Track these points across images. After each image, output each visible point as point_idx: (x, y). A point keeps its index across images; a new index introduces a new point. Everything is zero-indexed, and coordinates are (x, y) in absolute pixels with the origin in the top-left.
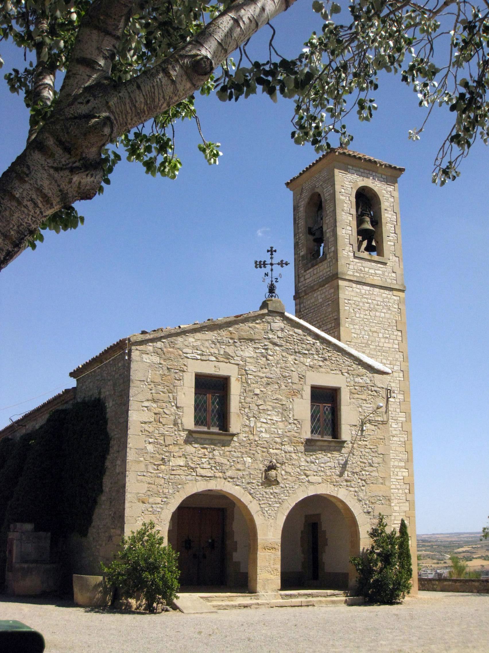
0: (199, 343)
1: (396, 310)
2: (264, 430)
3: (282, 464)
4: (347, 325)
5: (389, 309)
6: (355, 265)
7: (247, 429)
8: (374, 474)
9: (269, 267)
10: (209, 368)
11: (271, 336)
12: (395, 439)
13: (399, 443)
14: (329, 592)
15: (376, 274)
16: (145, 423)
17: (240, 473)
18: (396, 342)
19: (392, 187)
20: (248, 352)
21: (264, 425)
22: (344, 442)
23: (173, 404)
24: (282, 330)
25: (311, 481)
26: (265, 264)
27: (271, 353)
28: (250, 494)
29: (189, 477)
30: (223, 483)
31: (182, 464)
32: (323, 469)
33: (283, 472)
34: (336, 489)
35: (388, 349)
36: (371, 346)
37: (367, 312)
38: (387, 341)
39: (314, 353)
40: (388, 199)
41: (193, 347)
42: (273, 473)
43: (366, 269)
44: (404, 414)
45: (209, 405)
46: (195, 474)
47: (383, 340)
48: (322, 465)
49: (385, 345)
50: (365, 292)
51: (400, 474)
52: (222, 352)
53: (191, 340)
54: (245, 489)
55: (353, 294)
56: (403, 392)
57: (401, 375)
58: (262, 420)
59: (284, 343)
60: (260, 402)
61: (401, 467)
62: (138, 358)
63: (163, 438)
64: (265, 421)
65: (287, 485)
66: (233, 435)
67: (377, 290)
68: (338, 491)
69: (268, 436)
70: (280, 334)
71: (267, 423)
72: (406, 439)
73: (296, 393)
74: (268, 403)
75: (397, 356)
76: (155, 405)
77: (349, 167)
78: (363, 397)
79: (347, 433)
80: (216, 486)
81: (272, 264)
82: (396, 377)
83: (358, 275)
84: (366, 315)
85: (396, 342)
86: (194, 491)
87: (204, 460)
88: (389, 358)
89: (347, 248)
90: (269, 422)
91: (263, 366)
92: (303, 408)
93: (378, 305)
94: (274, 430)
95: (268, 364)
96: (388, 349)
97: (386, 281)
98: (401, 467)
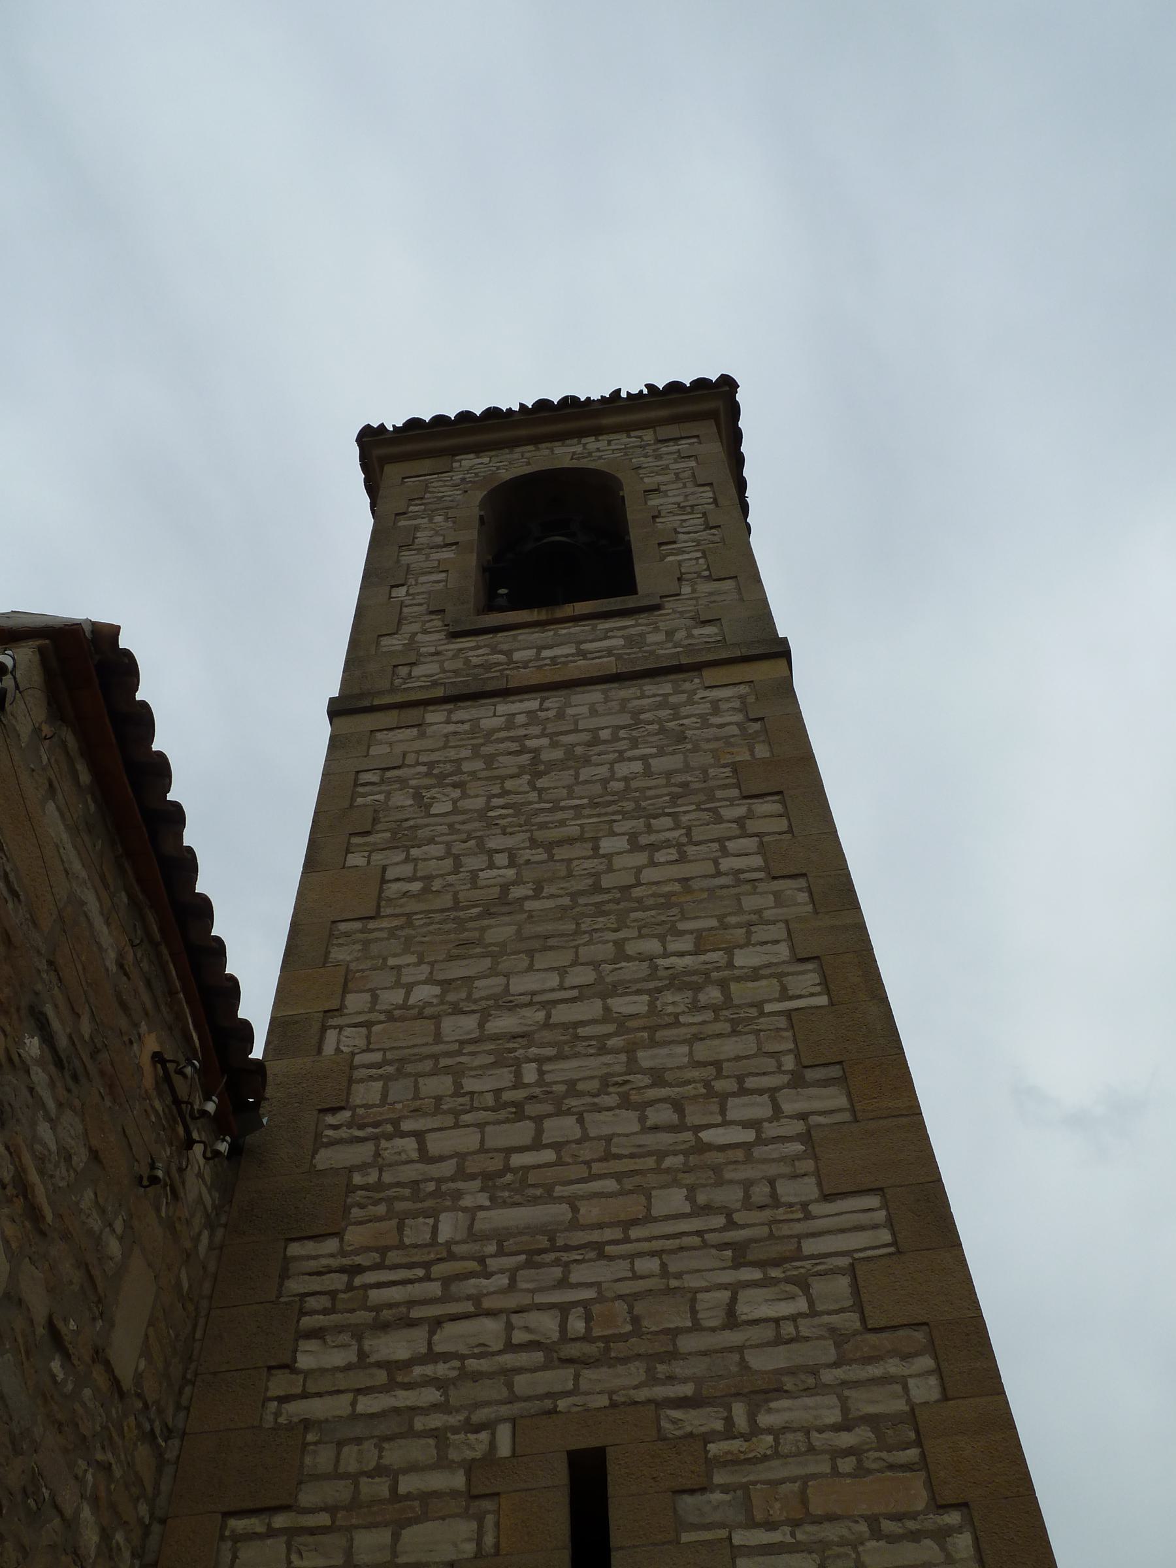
13: (846, 1439)
35: (677, 887)
44: (874, 1201)
56: (835, 1072)
57: (806, 980)
72: (925, 1390)
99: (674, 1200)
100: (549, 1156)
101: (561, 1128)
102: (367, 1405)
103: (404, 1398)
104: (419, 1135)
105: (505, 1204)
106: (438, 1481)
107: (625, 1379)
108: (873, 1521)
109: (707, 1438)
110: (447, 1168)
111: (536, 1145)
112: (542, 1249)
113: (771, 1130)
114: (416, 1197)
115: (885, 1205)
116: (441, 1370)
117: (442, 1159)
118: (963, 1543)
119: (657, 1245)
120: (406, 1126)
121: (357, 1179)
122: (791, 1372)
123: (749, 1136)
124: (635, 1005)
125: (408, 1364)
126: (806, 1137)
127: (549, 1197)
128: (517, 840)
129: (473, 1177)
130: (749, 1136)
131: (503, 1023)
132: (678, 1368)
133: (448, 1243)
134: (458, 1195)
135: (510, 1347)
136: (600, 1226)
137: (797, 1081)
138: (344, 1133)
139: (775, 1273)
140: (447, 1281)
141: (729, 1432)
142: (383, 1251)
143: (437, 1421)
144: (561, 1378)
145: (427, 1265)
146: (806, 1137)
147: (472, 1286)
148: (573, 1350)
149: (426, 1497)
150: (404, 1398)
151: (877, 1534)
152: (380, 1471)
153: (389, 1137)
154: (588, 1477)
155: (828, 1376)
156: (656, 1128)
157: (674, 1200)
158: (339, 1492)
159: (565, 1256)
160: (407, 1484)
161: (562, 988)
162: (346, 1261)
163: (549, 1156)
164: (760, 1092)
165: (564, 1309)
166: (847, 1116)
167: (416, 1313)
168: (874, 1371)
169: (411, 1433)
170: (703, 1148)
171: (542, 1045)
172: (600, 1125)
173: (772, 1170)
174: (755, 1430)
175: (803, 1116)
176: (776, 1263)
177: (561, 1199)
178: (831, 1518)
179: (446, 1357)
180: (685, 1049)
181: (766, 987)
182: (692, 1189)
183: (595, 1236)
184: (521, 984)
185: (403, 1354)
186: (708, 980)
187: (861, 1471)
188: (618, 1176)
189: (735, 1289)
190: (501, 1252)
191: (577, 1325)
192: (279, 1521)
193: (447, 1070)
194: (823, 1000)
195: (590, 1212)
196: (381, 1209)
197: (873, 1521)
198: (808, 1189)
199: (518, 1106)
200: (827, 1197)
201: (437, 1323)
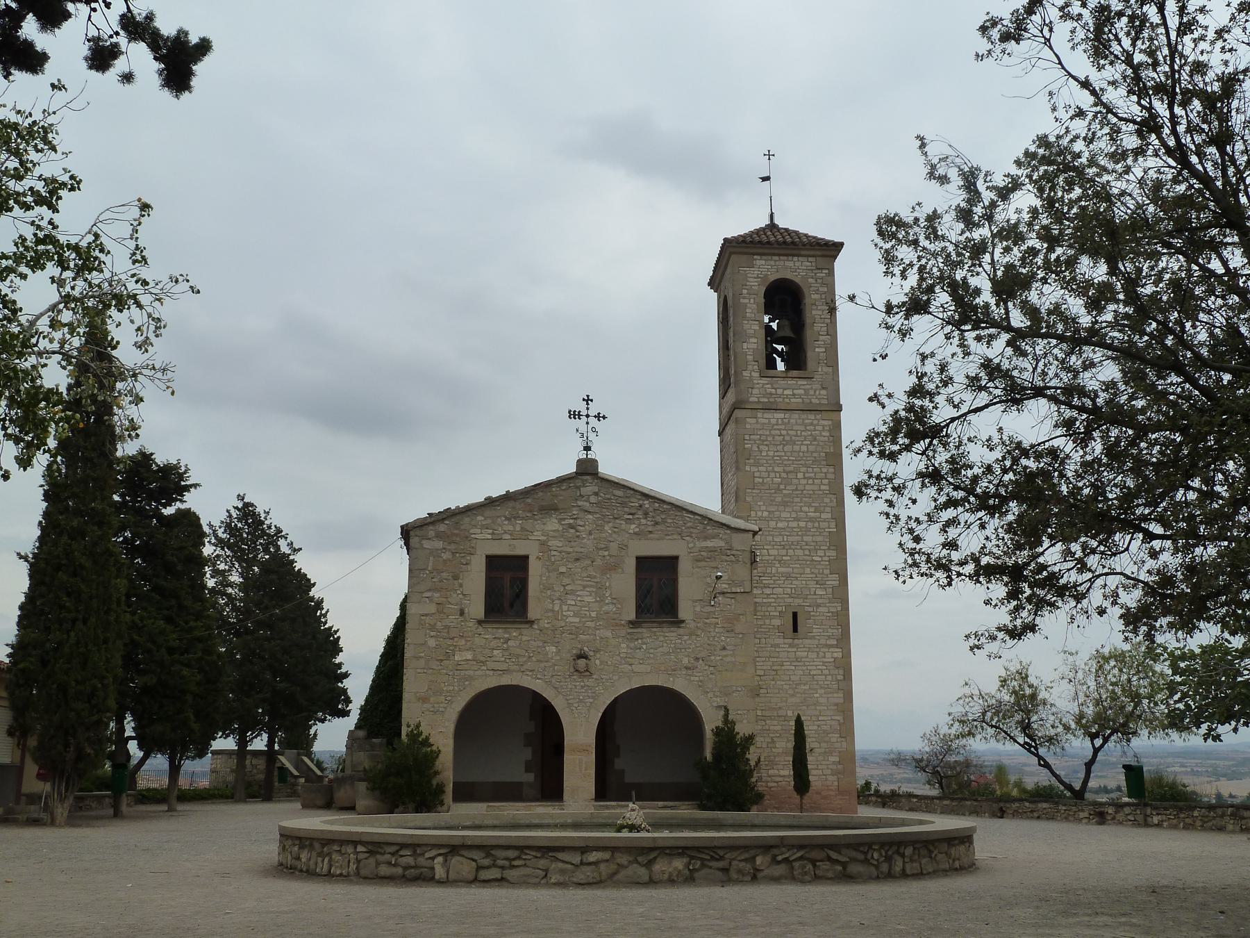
0: (489, 521)
3: (597, 651)
4: (748, 468)
5: (815, 439)
8: (729, 659)
9: (584, 418)
10: (500, 549)
11: (580, 503)
12: (821, 609)
14: (661, 804)
16: (426, 615)
17: (542, 665)
20: (552, 524)
22: (683, 621)
24: (596, 494)
26: (579, 415)
29: (479, 673)
31: (470, 657)
33: (598, 662)
38: (810, 481)
42: (582, 662)
43: (779, 391)
47: (804, 482)
49: (807, 487)
51: (828, 655)
52: (518, 528)
53: (480, 518)
55: (758, 426)
57: (833, 524)
59: (597, 509)
60: (566, 581)
61: (832, 646)
62: (417, 546)
66: (532, 622)
67: (796, 415)
70: (593, 499)
73: (612, 567)
75: (827, 500)
76: (437, 595)
78: (713, 564)
79: (684, 611)
81: (588, 416)
85: (826, 481)
89: (750, 367)
92: (625, 584)
98: (832, 646)
99: (808, 571)
101: (791, 552)
107: (799, 601)
112: (788, 576)
124: (802, 524)
131: (780, 525)
154: (795, 615)
157: (808, 571)
181: (826, 524)
184: (784, 515)
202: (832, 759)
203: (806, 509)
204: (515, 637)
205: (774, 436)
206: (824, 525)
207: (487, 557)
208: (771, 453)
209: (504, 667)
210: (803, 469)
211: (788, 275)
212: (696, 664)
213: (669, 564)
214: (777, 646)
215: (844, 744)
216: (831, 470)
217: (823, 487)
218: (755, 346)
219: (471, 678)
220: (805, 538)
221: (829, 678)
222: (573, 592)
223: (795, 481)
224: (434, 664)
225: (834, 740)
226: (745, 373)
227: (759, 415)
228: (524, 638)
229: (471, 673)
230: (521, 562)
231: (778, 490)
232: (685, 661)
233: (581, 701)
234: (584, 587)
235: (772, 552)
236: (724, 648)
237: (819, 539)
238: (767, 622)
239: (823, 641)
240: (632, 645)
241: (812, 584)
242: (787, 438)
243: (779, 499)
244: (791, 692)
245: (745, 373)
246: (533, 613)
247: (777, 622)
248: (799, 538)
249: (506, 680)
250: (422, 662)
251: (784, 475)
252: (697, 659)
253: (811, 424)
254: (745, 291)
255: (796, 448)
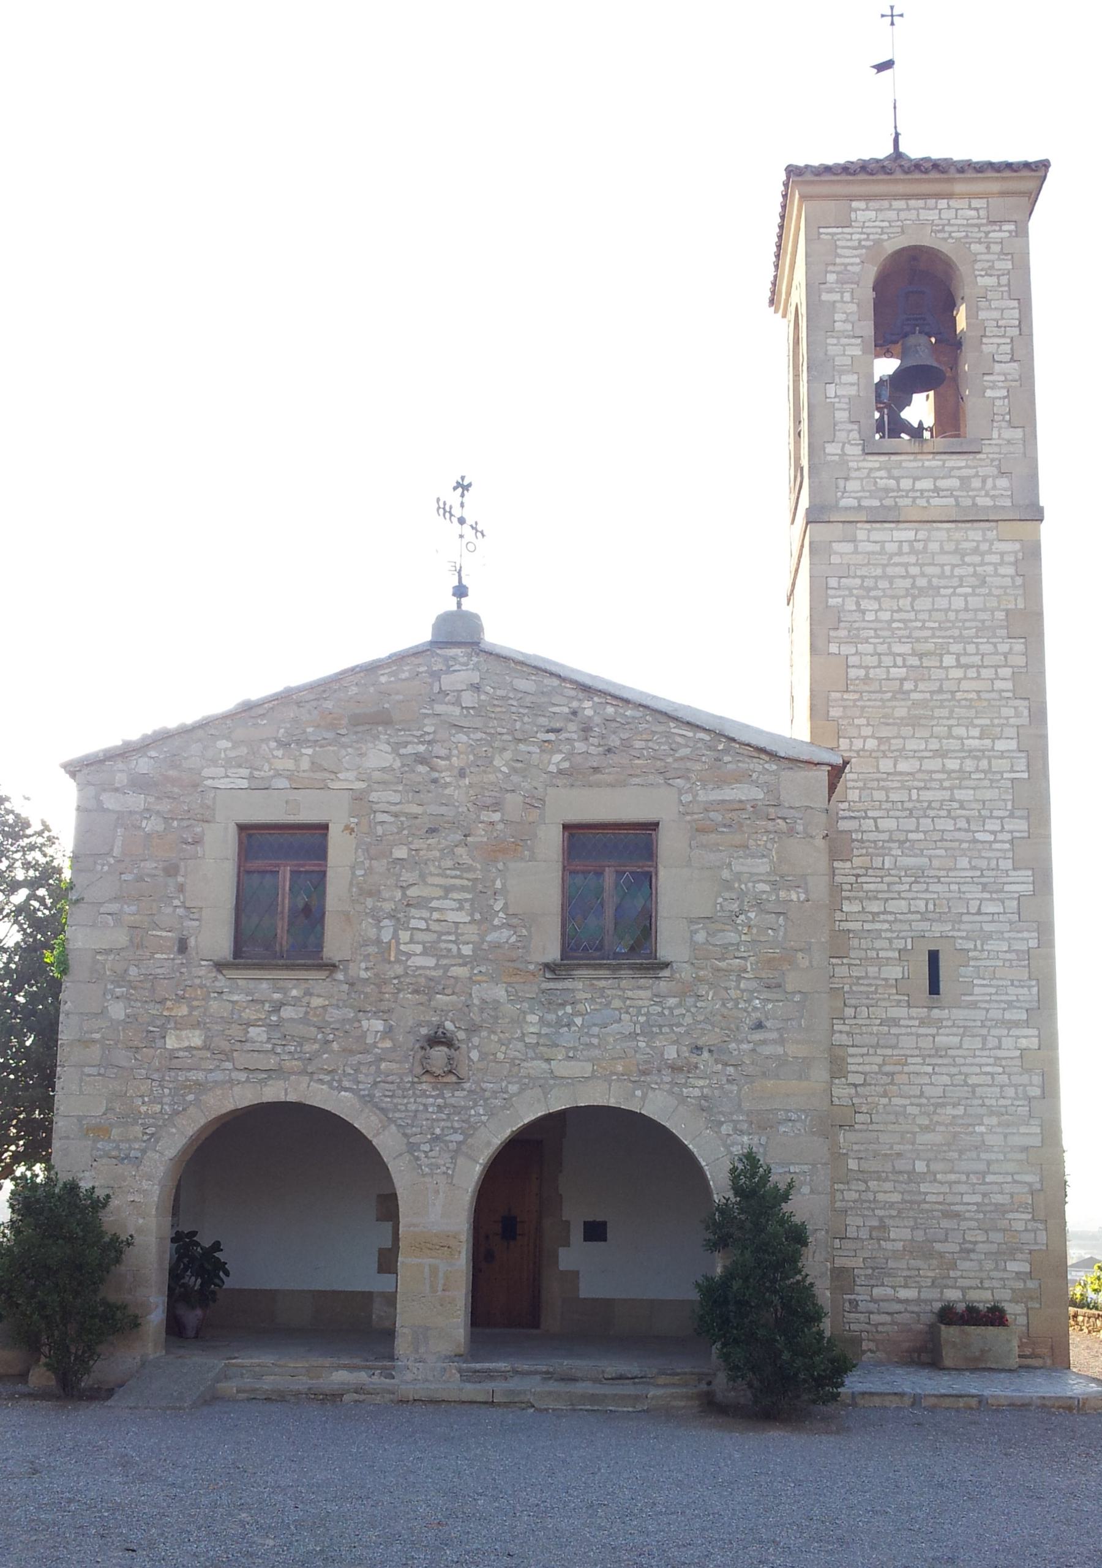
1: (1008, 581)
2: (419, 949)
3: (473, 1029)
4: (833, 648)
5: (983, 583)
6: (868, 476)
7: (372, 949)
12: (991, 945)
13: (1008, 956)
15: (936, 490)
17: (355, 1059)
18: (1006, 672)
19: (1006, 227)
21: (420, 936)
23: (176, 902)
25: (557, 1074)
27: (443, 752)
28: (382, 1109)
30: (305, 1085)
32: (595, 1041)
33: (475, 1055)
34: (638, 1093)
36: (914, 696)
37: (905, 603)
38: (972, 673)
39: (575, 736)
40: (992, 267)
41: (228, 760)
42: (439, 1053)
43: (906, 484)
44: (1030, 873)
45: (283, 895)
46: (231, 1067)
47: (958, 673)
48: (595, 1030)
49: (965, 685)
50: (900, 548)
51: (1008, 1042)
52: (305, 764)
54: (368, 1100)
56: (1025, 813)
57: (1021, 765)
58: (413, 923)
60: (407, 876)
61: (1016, 1024)
63: (148, 985)
64: (422, 925)
65: (484, 1085)
66: (332, 967)
67: (941, 532)
68: (644, 1096)
69: (431, 962)
71: (428, 929)
72: (1033, 943)
73: (511, 846)
74: (430, 880)
77: (854, 204)
79: (670, 942)
80: (286, 1094)
82: (1002, 773)
83: (877, 503)
84: (900, 610)
85: (1006, 672)
86: (229, 1106)
87: (253, 1031)
88: (977, 722)
89: (841, 436)
90: (434, 926)
91: (421, 787)
92: (538, 884)
93: (942, 576)
94: (450, 946)
95: (435, 781)
96: (973, 696)
97: (974, 504)
98: (1016, 1024)
99: (963, 862)
100: (921, 836)
101: (926, 823)
102: (867, 926)
103: (878, 926)
104: (875, 819)
105: (907, 856)
106: (890, 954)
108: (1012, 981)
109: (968, 951)
110: (885, 836)
111: (917, 831)
113: (1000, 837)
114: (875, 848)
115: (1033, 875)
116: (890, 918)
117: (883, 832)
118: (1035, 990)
119: (958, 880)
120: (870, 814)
121: (854, 836)
122: (996, 932)
123: (992, 838)
124: (952, 764)
125: (878, 913)
126: (1012, 842)
127: (922, 855)
128: (906, 649)
129: (895, 841)
130: (992, 838)
131: (903, 766)
132: (963, 927)
133: (889, 869)
134: (890, 849)
135: (910, 912)
136: (939, 869)
137: (1012, 816)
138: (847, 814)
139: (994, 896)
140: (889, 884)
141: (975, 949)
142: (867, 869)
143: (889, 935)
144: (925, 925)
145: (882, 877)
146: (1012, 842)
147: (897, 888)
148: (930, 916)
149: (888, 959)
150: (878, 926)
151: (1012, 985)
152: (873, 949)
153: (864, 818)
154: (934, 958)
155: (1006, 935)
156: (960, 829)
157: (963, 862)
158: (862, 954)
159: (927, 880)
160: (882, 954)
161: (926, 750)
162: (855, 872)
163: (921, 836)
164: (997, 818)
165: (927, 901)
166: (1026, 834)
167: (880, 896)
168: (1020, 935)
169: (881, 937)
170: (975, 841)
171: (919, 780)
172: (941, 824)
173: (999, 854)
174: (983, 950)
175: (1012, 832)
176: (996, 892)
177: (926, 856)
178: (1001, 979)
179: (891, 913)
180: (972, 792)
182: (971, 858)
183: (937, 873)
184: (912, 745)
185: (876, 910)
186: (984, 756)
187: (1011, 966)
188: (946, 849)
189: (981, 900)
190: (906, 876)
191: (931, 907)
192: (845, 961)
193: (883, 788)
194: (1026, 775)
195: (936, 863)
196: (864, 851)
197: (1012, 981)
198: (1009, 864)
199: (911, 811)
200: (1014, 869)
201: (887, 900)
202: (1013, 1267)
203: (961, 731)
204: (300, 995)
205: (892, 579)
206: (999, 764)
207: (242, 828)
208: (885, 616)
209: (272, 1062)
210: (956, 648)
211: (927, 240)
212: (694, 1059)
213: (636, 841)
214: (895, 1022)
215: (1042, 1237)
216: (1019, 647)
217: (999, 685)
218: (853, 391)
219: (201, 1087)
220: (959, 794)
221: (1010, 1092)
222: (421, 903)
223: (939, 674)
224: (121, 1057)
225: (1019, 1226)
226: (831, 449)
227: (861, 535)
228: (316, 1002)
229: (200, 1076)
230: (310, 840)
231: (901, 693)
232: (671, 1053)
233: (437, 1139)
234: (448, 890)
235: (890, 824)
236: (759, 1026)
237: (989, 794)
238: (872, 970)
239: (995, 1014)
240: (551, 1017)
241: (974, 892)
242: (922, 582)
243: (901, 712)
244: (924, 1121)
245: (831, 449)
246: (334, 946)
247: (894, 972)
248: (946, 794)
249: (273, 1092)
250: (96, 1051)
251: (914, 661)
252: (698, 1049)
253: (975, 551)
254: (831, 278)
255: (942, 603)
